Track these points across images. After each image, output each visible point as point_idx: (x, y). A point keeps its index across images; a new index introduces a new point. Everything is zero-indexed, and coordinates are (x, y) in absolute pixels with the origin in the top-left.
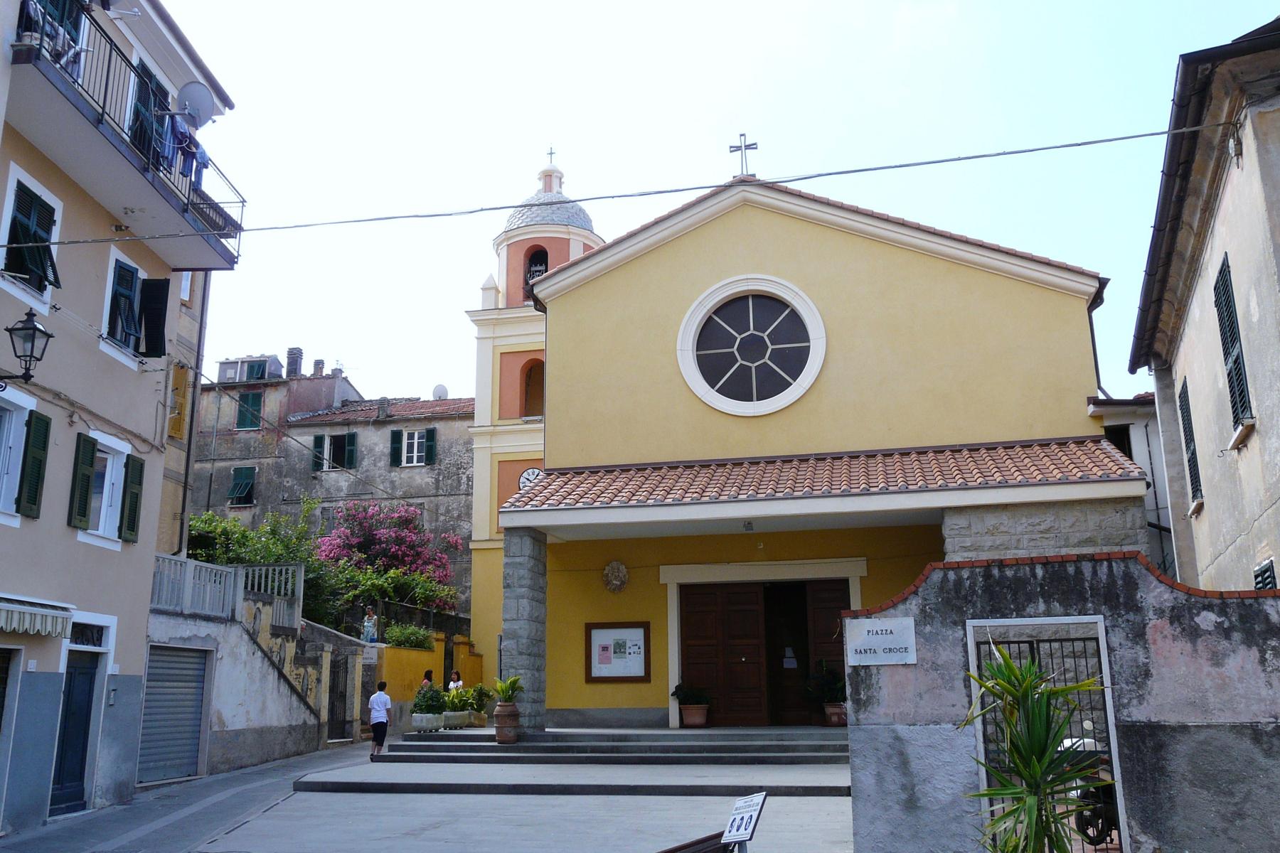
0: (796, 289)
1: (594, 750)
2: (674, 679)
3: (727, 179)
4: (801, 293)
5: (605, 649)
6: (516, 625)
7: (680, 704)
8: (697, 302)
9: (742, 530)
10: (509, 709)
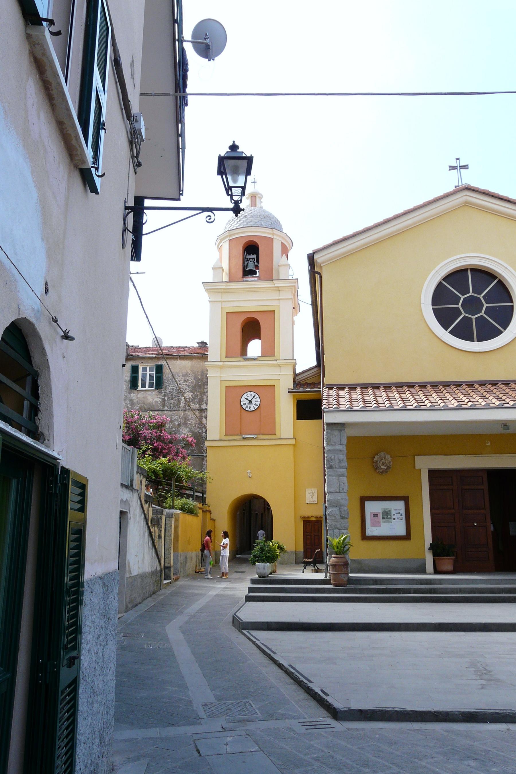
0: (506, 265)
1: (416, 591)
2: (428, 539)
3: (452, 189)
4: (509, 268)
5: (376, 515)
6: (338, 497)
7: (434, 556)
8: (434, 272)
9: (501, 431)
10: (343, 560)
